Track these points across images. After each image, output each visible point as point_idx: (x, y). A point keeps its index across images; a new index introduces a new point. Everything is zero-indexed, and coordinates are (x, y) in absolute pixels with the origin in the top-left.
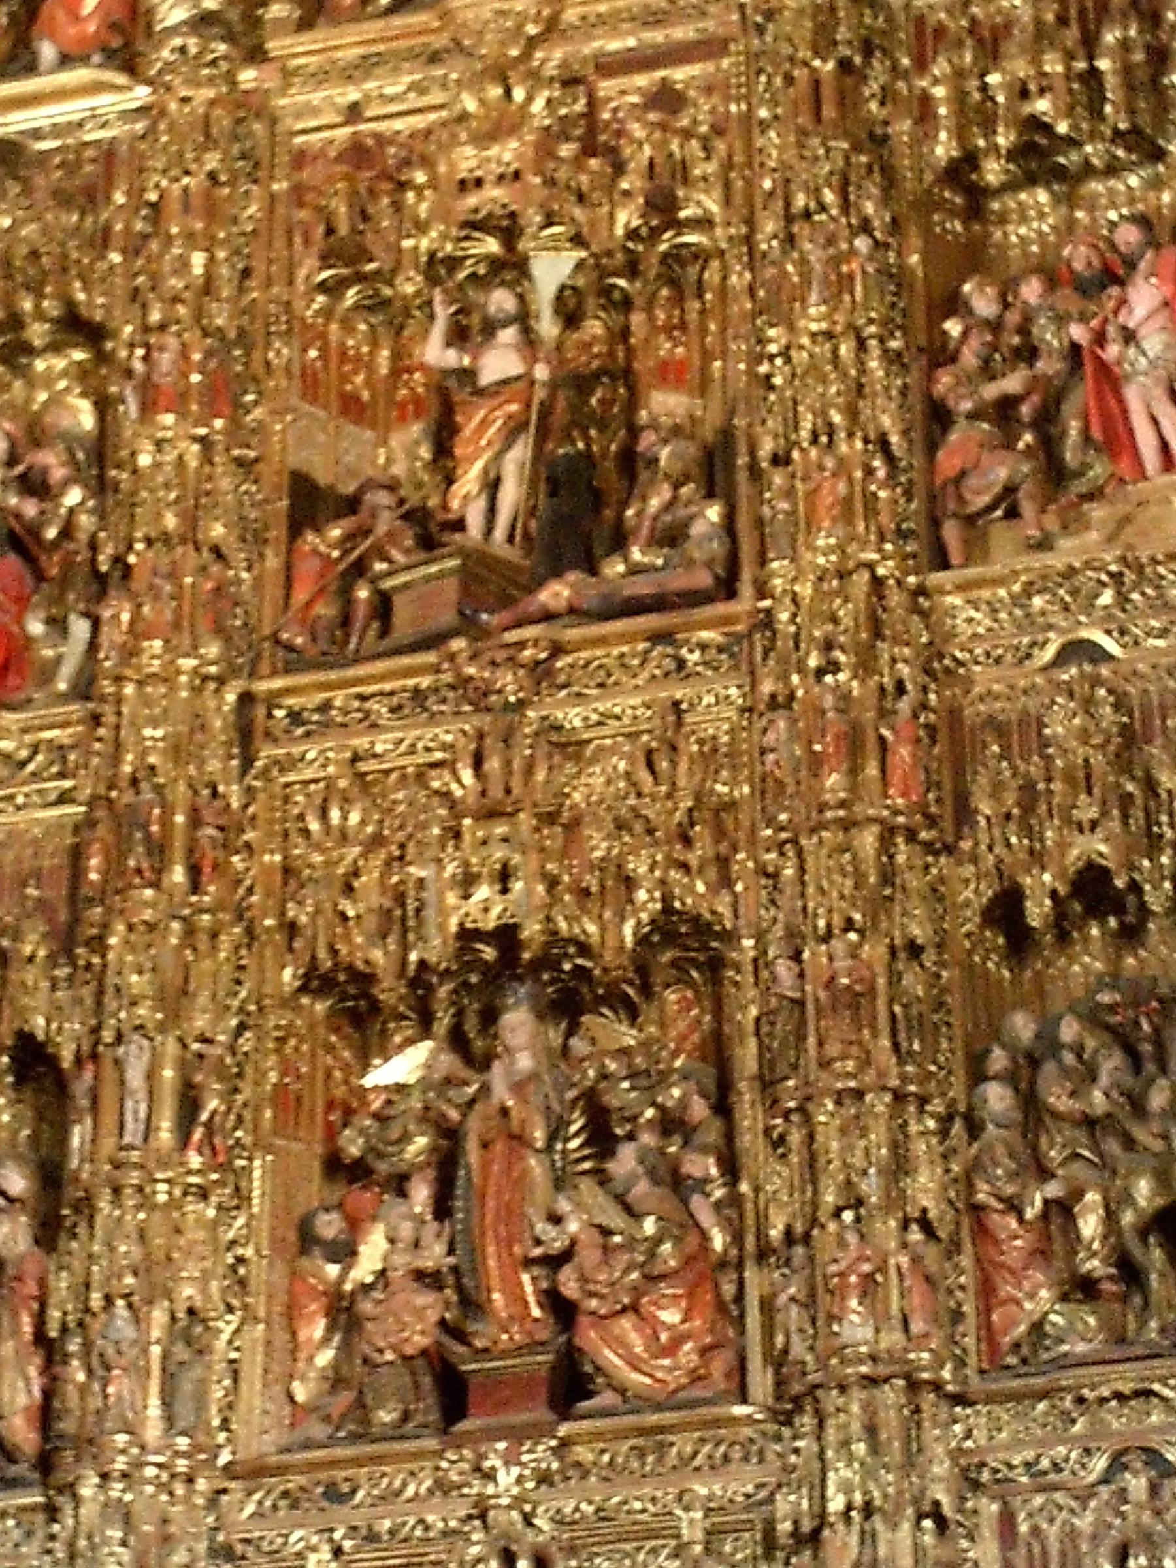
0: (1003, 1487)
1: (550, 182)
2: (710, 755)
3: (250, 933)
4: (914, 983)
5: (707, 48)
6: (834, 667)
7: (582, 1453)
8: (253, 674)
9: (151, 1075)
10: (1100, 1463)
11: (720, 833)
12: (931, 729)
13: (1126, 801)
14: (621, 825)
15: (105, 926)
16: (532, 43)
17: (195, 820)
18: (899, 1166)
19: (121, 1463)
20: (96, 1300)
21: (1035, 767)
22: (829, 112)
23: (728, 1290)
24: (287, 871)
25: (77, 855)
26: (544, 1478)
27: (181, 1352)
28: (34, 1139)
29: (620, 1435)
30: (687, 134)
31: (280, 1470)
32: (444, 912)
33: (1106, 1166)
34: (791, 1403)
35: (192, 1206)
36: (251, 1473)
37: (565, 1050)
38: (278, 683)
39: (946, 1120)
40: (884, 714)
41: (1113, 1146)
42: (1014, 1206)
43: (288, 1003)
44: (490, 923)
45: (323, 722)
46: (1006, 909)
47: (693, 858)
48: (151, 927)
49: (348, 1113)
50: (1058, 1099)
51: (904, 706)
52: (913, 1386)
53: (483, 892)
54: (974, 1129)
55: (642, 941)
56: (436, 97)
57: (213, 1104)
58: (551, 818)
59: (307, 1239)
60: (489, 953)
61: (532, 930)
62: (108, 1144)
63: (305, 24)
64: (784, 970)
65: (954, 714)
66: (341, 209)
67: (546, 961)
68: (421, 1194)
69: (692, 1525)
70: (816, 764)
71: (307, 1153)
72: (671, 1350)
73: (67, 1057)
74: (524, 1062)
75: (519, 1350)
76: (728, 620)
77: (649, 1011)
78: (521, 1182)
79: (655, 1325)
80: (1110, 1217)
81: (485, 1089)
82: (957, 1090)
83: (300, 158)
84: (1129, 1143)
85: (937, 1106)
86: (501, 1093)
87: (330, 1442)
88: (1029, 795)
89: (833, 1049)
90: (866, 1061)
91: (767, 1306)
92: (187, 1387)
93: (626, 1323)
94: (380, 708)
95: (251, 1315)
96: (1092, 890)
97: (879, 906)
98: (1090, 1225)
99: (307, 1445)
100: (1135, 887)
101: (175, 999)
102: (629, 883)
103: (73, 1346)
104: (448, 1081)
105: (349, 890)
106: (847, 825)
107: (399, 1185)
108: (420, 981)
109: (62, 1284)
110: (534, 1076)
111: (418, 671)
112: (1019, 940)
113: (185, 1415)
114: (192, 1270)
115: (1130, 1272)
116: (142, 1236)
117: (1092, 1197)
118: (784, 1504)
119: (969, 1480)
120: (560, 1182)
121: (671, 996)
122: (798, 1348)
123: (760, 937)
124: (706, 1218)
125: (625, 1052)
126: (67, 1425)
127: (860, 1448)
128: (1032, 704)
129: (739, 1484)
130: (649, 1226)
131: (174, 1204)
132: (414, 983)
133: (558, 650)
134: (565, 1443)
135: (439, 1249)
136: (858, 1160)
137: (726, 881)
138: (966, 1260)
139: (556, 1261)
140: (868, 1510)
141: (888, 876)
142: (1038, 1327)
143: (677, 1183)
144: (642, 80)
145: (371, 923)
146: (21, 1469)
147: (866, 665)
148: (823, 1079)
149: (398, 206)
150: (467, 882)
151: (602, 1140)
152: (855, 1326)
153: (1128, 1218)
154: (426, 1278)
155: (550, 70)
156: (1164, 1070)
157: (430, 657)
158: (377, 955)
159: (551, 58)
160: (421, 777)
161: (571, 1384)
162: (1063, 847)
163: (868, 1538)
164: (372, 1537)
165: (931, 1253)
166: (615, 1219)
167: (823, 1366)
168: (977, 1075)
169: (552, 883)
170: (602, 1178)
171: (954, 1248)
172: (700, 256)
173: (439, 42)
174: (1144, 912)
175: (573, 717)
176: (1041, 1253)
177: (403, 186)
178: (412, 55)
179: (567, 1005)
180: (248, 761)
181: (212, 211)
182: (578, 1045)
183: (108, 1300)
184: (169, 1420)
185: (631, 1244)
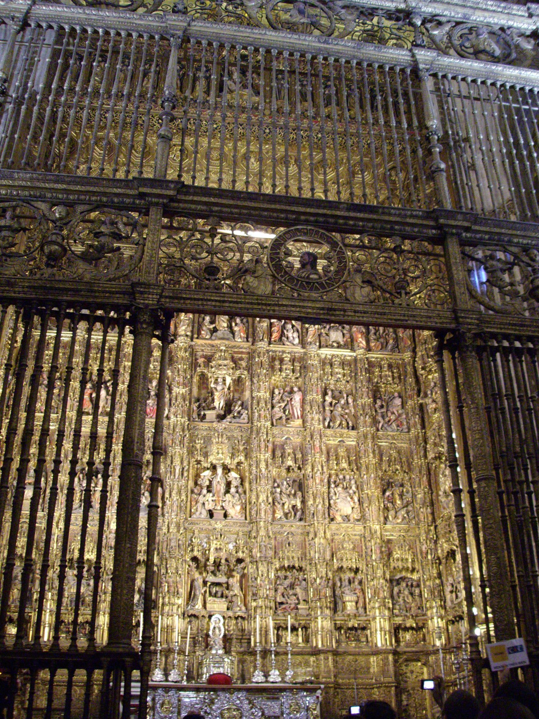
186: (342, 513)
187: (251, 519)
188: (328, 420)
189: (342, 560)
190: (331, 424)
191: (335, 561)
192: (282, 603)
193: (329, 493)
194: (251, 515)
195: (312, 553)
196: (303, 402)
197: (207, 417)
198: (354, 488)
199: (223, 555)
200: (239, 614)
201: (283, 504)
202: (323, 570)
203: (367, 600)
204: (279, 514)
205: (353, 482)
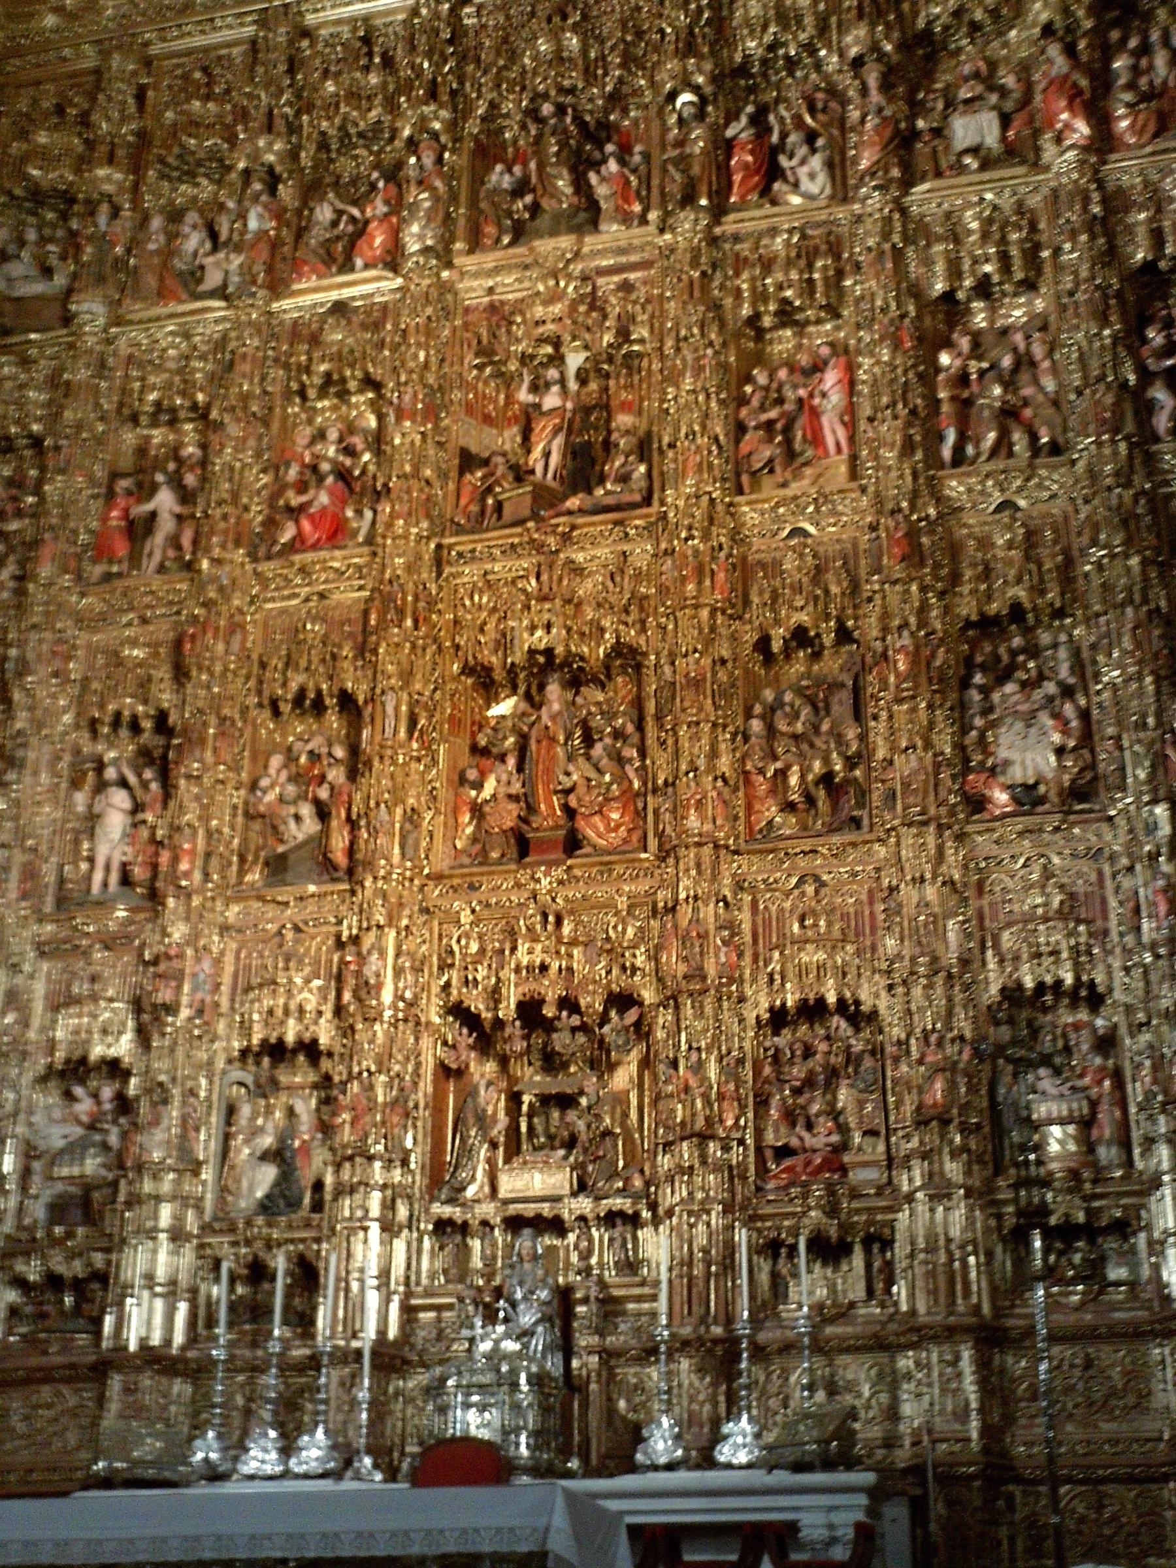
0: (753, 889)
1: (575, 322)
2: (638, 576)
3: (440, 648)
4: (722, 676)
5: (645, 265)
6: (692, 537)
7: (577, 872)
8: (443, 536)
9: (397, 709)
10: (794, 880)
11: (642, 609)
12: (734, 566)
13: (816, 598)
14: (599, 605)
15: (378, 644)
16: (569, 261)
17: (416, 598)
18: (714, 754)
19: (382, 873)
20: (372, 803)
21: (777, 582)
22: (697, 294)
23: (640, 805)
24: (456, 622)
25: (366, 614)
26: (561, 882)
27: (408, 826)
28: (348, 735)
29: (593, 865)
30: (635, 302)
31: (451, 877)
32: (522, 642)
33: (801, 755)
34: (666, 853)
35: (414, 765)
36: (438, 877)
37: (574, 703)
38: (453, 540)
39: (734, 735)
40: (714, 558)
41: (805, 747)
42: (761, 771)
43: (456, 679)
44: (542, 646)
45: (470, 557)
46: (763, 644)
47: (630, 620)
48: (397, 645)
49: (481, 727)
50: (782, 726)
51: (722, 554)
52: (716, 847)
53: (539, 633)
54: (746, 739)
55: (607, 656)
56: (527, 284)
57: (422, 722)
58: (569, 601)
59: (462, 780)
60: (541, 659)
61: (560, 650)
62: (378, 738)
63: (471, 251)
64: (667, 669)
65: (744, 559)
66: (484, 332)
67: (567, 663)
68: (511, 762)
69: (622, 903)
70: (684, 580)
71: (464, 743)
72: (616, 829)
73: (361, 700)
74: (556, 707)
75: (552, 829)
76: (647, 516)
77: (610, 686)
78: (553, 758)
79: (609, 820)
80: (803, 777)
81: (539, 718)
82: (740, 721)
83: (467, 310)
84: (812, 745)
85: (730, 728)
86: (545, 719)
87: (472, 865)
88: (775, 596)
89: (687, 704)
90: (701, 709)
91: (656, 812)
92: (410, 841)
93: (597, 818)
94: (497, 552)
95: (438, 812)
96: (800, 637)
97: (709, 642)
98: (794, 780)
99: (462, 866)
100: (818, 635)
101: (407, 676)
102: (602, 630)
103: (363, 823)
104: (524, 714)
105: (482, 630)
106: (696, 607)
107: (502, 758)
108: (512, 671)
109: (358, 797)
110: (560, 713)
111: (514, 535)
112: (769, 658)
113: (410, 852)
114: (413, 792)
115: (810, 800)
116: (392, 776)
117: (795, 768)
118: (660, 895)
119: (739, 886)
120: (570, 758)
121: (620, 679)
122: (668, 830)
123: (657, 654)
124: (631, 774)
125: (598, 704)
126: (359, 856)
127: (693, 872)
128: (778, 555)
129: (643, 886)
130: (607, 778)
131: (405, 764)
132: (509, 672)
133: (573, 527)
134: (570, 868)
135: (518, 785)
136: (696, 750)
137: (644, 630)
138: (741, 794)
139: (568, 792)
140: (696, 898)
141: (713, 629)
142: (770, 822)
143: (620, 760)
144: (616, 279)
145: (491, 645)
146: (341, 874)
147: (706, 537)
148: (683, 717)
149: (509, 332)
150: (532, 629)
151: (589, 740)
152: (693, 821)
153: (810, 777)
154: (512, 798)
155: (577, 273)
156: (828, 713)
157: (519, 530)
158: (494, 659)
159: (577, 268)
160: (514, 582)
161: (573, 843)
162: (788, 617)
163: (696, 910)
164: (488, 905)
165: (726, 790)
166: (592, 774)
167: (679, 837)
168: (748, 715)
169: (569, 630)
170: (588, 758)
171: (736, 789)
172: (640, 355)
173: (529, 260)
174: (822, 647)
175: (580, 557)
176: (773, 792)
177: (511, 323)
178: (517, 266)
179: (575, 682)
180: (439, 574)
181: (429, 333)
182: (579, 700)
183: (378, 804)
184: (403, 855)
185: (599, 785)
186: (1017, 774)
187: (660, 845)
188: (951, 436)
189: (1016, 958)
190: (970, 450)
191: (992, 964)
192: (783, 1152)
193: (962, 706)
194: (660, 835)
195: (891, 943)
196: (851, 385)
197: (507, 510)
198: (1064, 672)
199: (551, 990)
200: (618, 1203)
201: (782, 773)
202: (927, 1004)
203: (1133, 1110)
204: (770, 811)
205: (1063, 653)
